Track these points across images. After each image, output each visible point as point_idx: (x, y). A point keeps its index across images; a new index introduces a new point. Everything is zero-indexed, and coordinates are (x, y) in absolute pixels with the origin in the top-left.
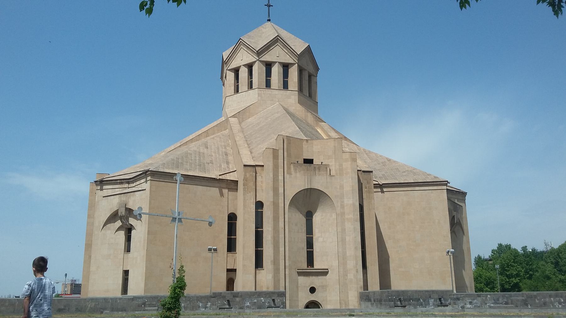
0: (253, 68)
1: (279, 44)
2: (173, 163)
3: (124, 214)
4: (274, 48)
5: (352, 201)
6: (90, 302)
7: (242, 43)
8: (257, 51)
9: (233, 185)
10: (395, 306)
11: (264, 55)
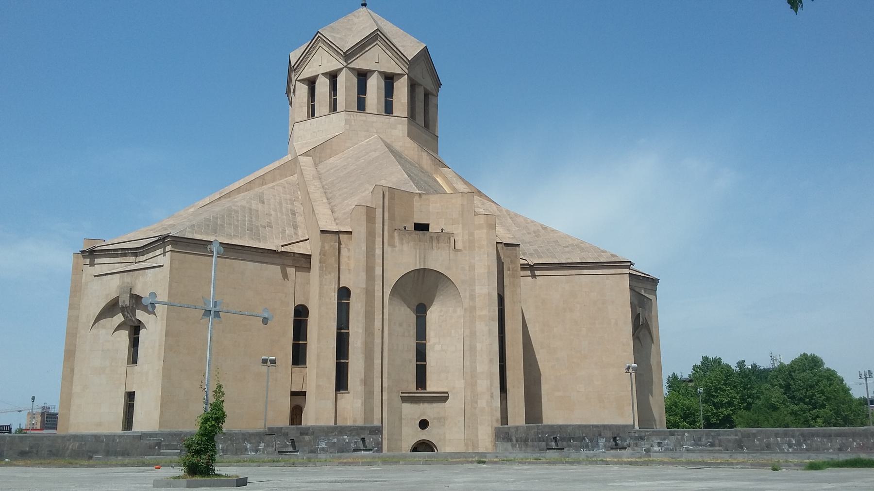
0: (338, 79)
1: (379, 43)
2: (208, 225)
3: (127, 303)
4: (371, 48)
5: (487, 289)
7: (321, 38)
8: (344, 53)
9: (303, 262)
10: (548, 449)
11: (356, 59)
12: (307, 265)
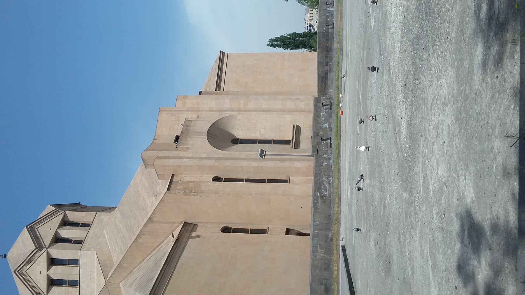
0: (55, 257)
1: (37, 227)
6: (317, 254)
8: (36, 248)
12: (192, 226)
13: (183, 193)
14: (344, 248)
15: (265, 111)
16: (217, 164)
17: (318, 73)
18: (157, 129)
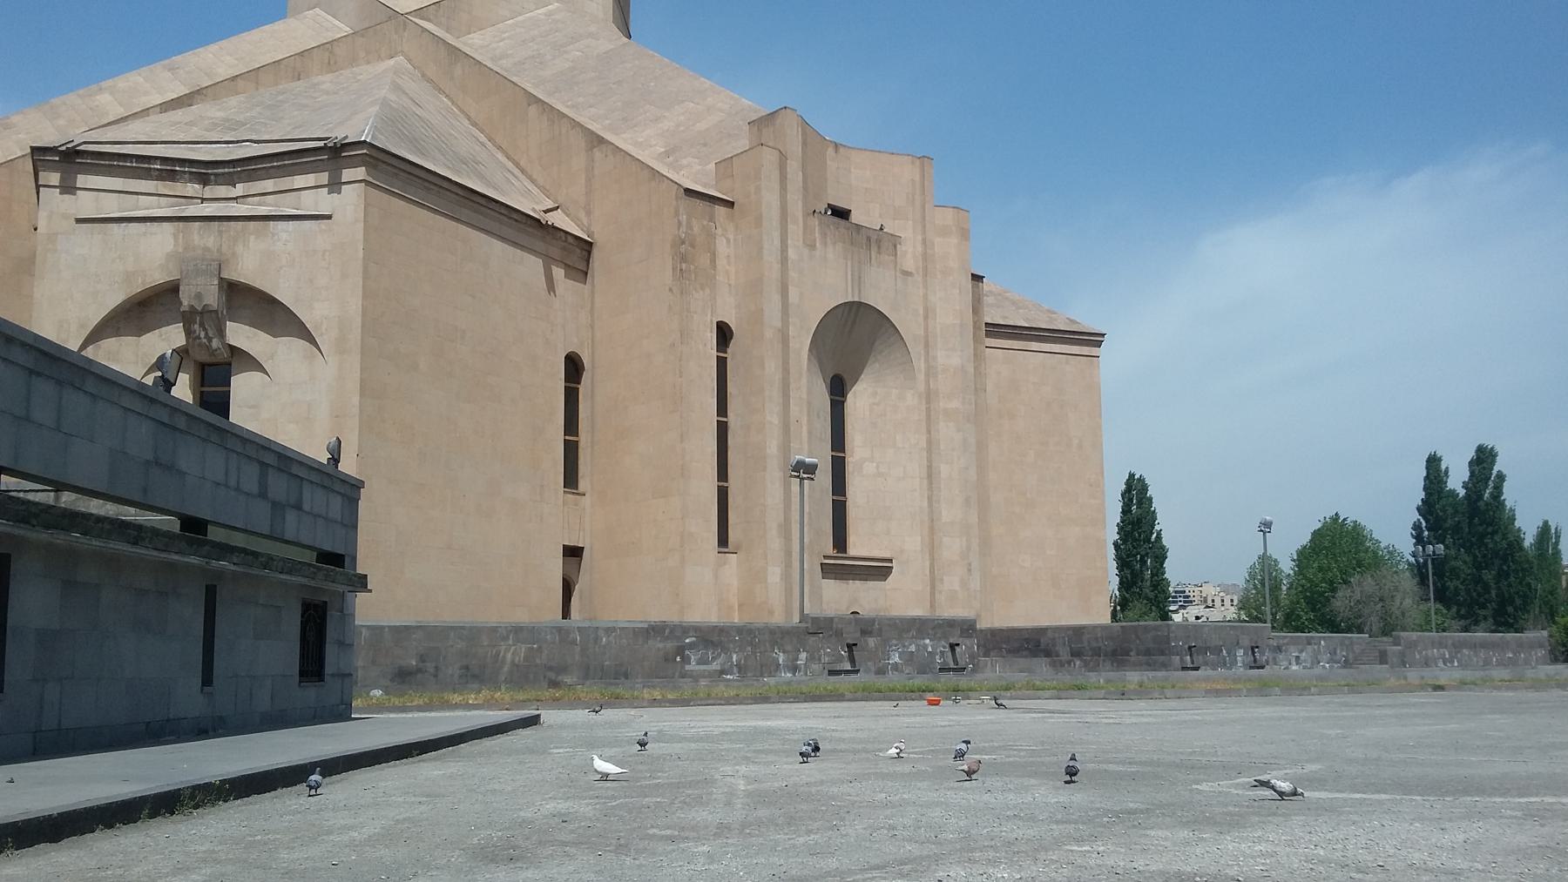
6: (511, 642)
13: (680, 238)
14: (533, 721)
15: (931, 475)
16: (769, 334)
17: (1047, 629)
18: (868, 153)
